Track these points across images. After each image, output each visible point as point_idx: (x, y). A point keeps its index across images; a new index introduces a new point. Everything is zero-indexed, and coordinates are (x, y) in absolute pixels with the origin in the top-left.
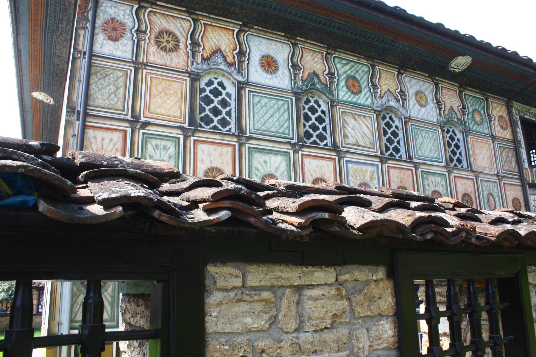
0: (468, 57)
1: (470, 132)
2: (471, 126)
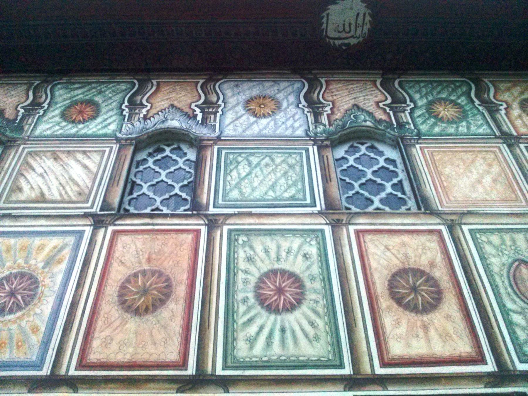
1: (420, 138)
2: (424, 128)
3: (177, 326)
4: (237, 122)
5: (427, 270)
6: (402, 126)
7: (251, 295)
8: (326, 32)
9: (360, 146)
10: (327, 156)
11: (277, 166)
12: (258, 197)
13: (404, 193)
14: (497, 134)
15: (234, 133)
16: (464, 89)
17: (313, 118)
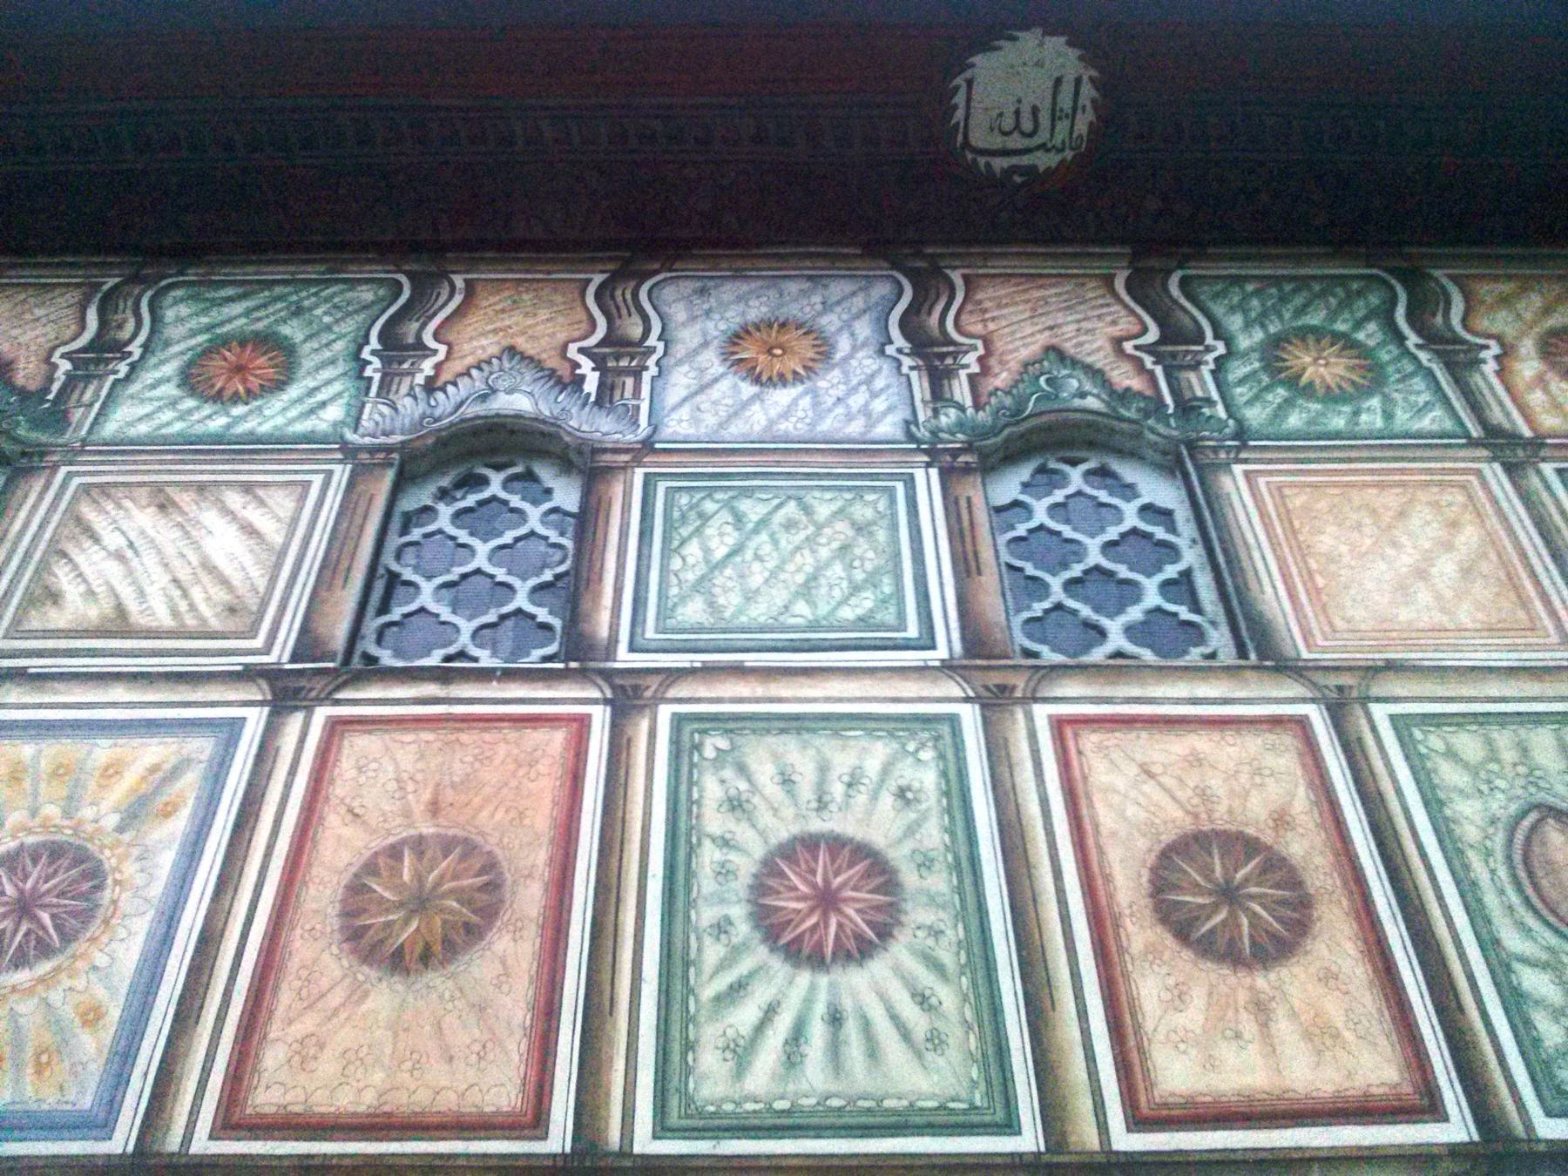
0: (1029, 41)
1: (1244, 447)
2: (1255, 416)
3: (516, 1006)
4: (698, 398)
5: (1267, 838)
6: (1193, 408)
7: (738, 912)
8: (966, 136)
9: (1066, 468)
10: (969, 500)
11: (820, 527)
12: (762, 619)
13: (1197, 608)
14: (1475, 434)
15: (692, 431)
16: (1374, 300)
17: (926, 385)
